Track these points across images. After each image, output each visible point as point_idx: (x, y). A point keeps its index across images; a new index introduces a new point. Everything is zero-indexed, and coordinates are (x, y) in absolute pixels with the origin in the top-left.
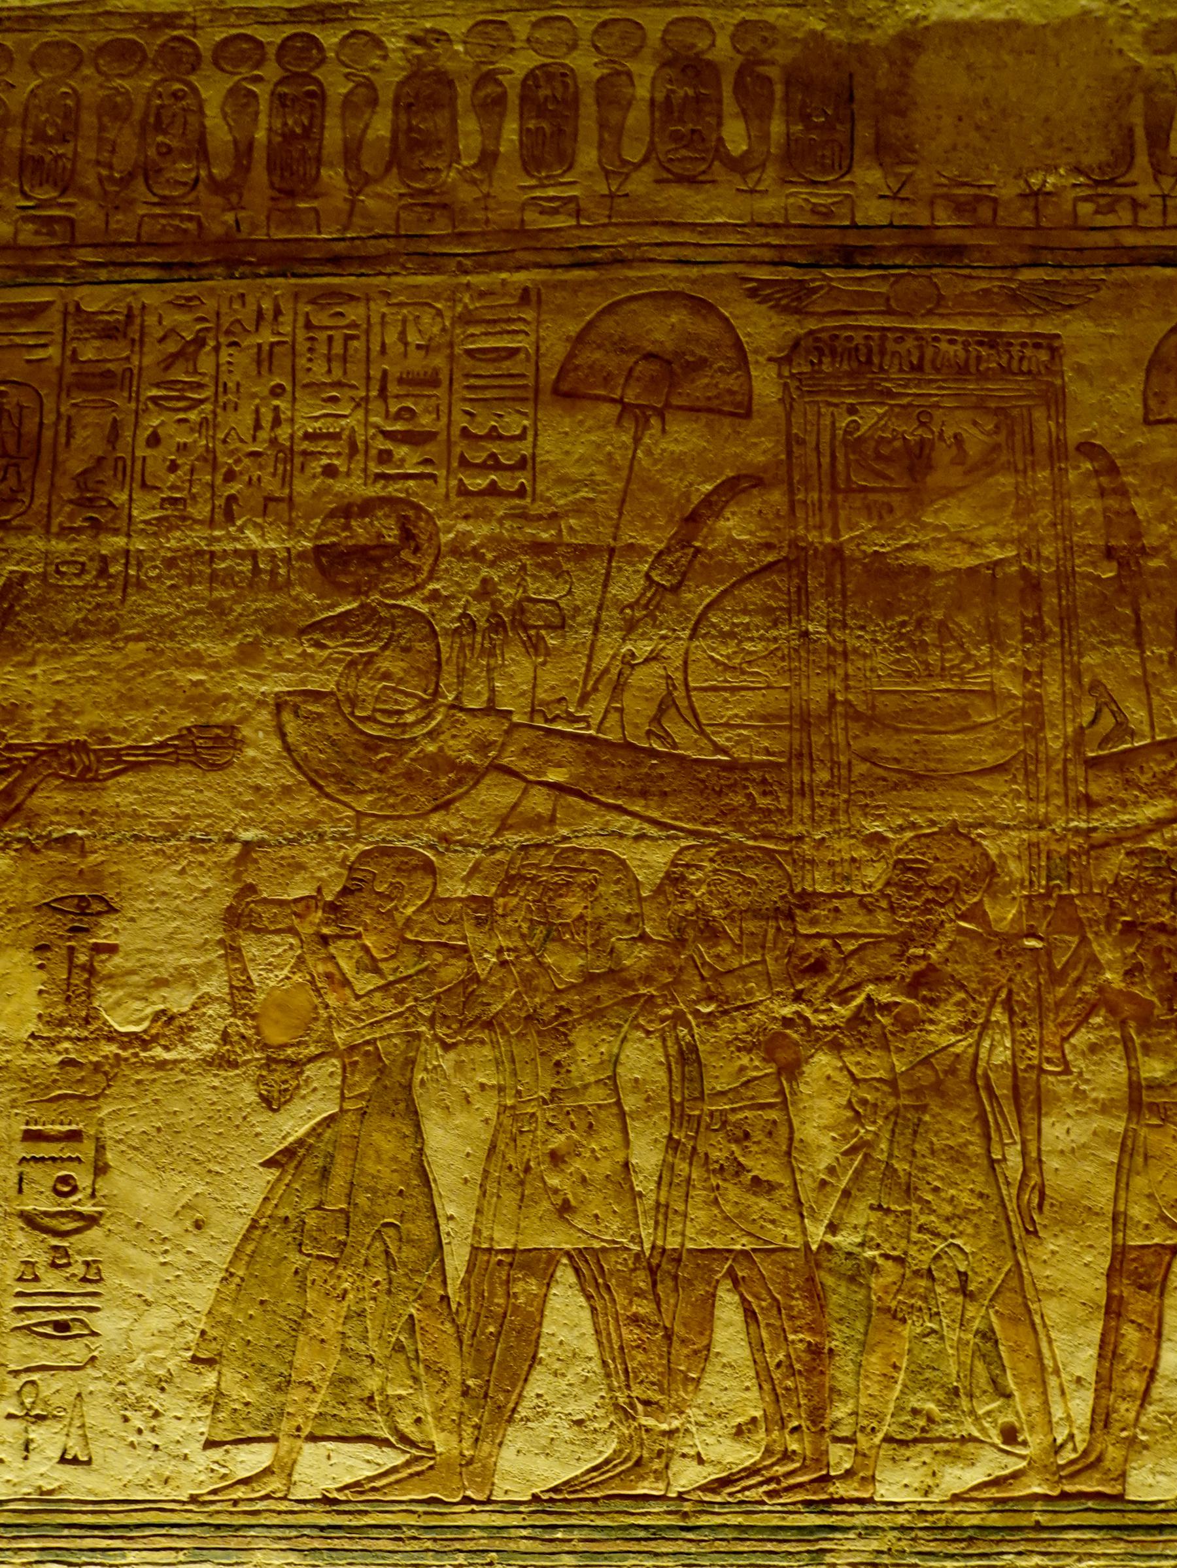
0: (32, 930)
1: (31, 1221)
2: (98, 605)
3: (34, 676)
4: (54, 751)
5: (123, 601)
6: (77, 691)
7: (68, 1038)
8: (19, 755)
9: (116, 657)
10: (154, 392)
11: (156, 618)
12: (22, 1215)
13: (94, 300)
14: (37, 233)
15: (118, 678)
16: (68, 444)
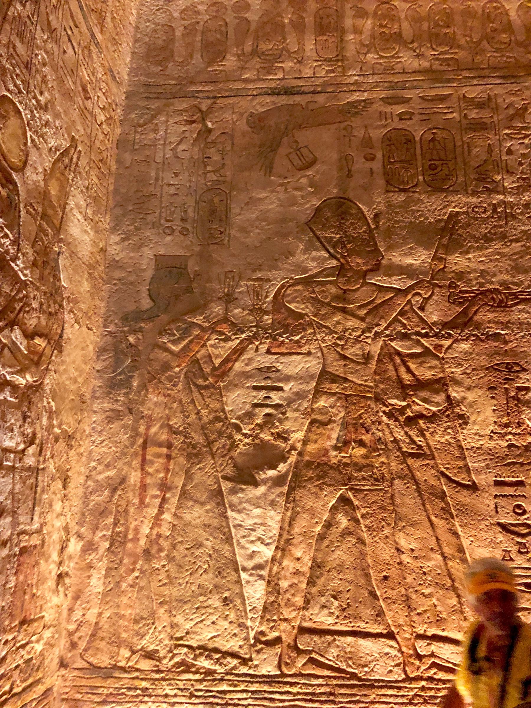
0: (486, 379)
1: (504, 527)
2: (495, 226)
3: (469, 259)
4: (483, 293)
5: (506, 224)
6: (491, 265)
7: (510, 433)
8: (467, 295)
9: (507, 250)
10: (507, 131)
11: (522, 231)
12: (499, 524)
13: (472, 93)
14: (441, 65)
15: (510, 259)
16: (469, 154)
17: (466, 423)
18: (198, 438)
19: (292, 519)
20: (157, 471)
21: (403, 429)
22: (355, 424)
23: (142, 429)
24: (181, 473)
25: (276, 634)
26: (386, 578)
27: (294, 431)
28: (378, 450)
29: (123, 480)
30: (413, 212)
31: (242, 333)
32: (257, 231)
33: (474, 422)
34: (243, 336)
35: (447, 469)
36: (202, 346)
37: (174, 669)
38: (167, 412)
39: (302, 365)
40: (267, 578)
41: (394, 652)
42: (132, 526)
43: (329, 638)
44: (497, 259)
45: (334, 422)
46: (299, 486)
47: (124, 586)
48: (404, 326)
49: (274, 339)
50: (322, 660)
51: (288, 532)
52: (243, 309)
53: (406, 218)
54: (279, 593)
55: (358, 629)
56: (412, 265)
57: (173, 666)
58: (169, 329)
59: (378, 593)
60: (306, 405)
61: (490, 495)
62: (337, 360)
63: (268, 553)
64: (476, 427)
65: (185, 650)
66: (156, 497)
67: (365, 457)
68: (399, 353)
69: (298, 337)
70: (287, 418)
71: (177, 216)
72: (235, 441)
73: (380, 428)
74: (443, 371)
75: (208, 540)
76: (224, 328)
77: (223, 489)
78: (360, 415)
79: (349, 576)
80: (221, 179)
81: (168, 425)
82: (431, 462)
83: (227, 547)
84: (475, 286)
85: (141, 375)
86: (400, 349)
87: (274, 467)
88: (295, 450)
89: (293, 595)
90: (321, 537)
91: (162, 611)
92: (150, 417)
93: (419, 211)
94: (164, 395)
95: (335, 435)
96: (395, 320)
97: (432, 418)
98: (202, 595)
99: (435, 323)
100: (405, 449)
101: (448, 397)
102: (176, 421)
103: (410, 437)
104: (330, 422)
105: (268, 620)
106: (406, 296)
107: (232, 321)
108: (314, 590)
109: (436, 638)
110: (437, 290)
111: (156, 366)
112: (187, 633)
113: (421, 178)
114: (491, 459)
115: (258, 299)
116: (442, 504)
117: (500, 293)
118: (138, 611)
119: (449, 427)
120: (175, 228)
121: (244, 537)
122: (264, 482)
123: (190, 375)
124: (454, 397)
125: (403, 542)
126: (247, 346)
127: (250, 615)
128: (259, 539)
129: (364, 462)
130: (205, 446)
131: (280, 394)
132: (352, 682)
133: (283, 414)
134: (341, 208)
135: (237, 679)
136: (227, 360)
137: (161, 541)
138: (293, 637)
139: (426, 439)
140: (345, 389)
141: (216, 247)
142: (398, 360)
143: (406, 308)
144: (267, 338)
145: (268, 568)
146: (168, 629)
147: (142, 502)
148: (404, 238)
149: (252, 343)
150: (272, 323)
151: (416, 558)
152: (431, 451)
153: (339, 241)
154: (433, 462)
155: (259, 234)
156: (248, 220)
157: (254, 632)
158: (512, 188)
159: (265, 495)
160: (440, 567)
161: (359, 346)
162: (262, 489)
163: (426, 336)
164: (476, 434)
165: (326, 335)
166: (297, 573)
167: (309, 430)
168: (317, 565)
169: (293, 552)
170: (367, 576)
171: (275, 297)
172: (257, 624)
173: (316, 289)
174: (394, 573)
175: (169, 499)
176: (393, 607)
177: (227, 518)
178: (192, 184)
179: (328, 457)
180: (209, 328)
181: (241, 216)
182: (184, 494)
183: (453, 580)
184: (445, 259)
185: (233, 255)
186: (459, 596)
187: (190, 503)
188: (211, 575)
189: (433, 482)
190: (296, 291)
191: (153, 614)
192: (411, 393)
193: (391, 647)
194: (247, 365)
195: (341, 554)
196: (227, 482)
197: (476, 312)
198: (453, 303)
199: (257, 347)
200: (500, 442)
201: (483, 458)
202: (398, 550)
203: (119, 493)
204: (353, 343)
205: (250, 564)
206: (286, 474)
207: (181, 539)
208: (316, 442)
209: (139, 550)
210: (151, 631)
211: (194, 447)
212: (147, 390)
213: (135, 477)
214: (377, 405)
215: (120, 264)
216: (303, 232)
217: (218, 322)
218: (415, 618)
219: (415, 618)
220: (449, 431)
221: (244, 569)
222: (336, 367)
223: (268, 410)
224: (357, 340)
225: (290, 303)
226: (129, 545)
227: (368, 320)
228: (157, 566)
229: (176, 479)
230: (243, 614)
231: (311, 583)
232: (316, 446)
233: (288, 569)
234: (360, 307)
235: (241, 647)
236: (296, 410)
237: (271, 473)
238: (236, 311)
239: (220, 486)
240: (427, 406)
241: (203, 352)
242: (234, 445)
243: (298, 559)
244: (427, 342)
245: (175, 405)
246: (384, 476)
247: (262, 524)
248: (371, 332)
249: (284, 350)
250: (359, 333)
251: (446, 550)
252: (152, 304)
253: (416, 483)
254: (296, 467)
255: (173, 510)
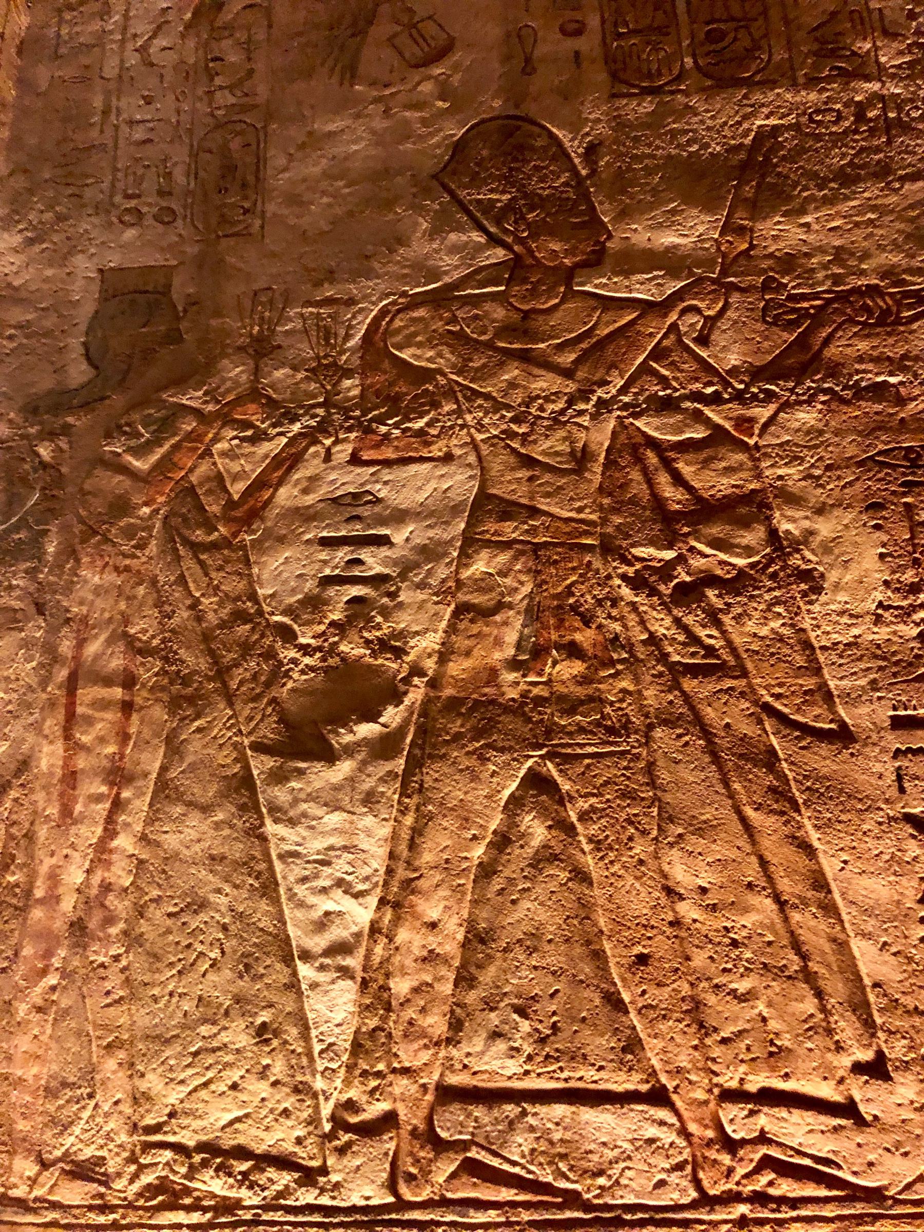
0: (858, 486)
2: (863, 149)
3: (807, 225)
5: (889, 142)
6: (859, 234)
9: (893, 199)
12: (909, 818)
15: (900, 218)
17: (818, 590)
18: (193, 660)
19: (417, 832)
20: (102, 740)
21: (670, 612)
22: (559, 607)
23: (66, 647)
24: (156, 741)
25: (382, 1107)
26: (642, 959)
27: (417, 633)
28: (612, 663)
29: (24, 765)
30: (674, 134)
31: (292, 421)
32: (325, 200)
33: (837, 586)
34: (296, 427)
35: (778, 697)
36: (201, 457)
37: (141, 1202)
38: (123, 605)
39: (433, 484)
40: (359, 975)
41: (668, 1137)
42: (44, 869)
43: (511, 1110)
44: (871, 221)
45: (510, 606)
46: (431, 756)
47: (22, 1009)
48: (664, 382)
49: (368, 431)
50: (495, 1162)
51: (408, 863)
52: (295, 368)
53: (658, 148)
54: (388, 1008)
55: (580, 1085)
56: (676, 247)
57: (140, 1195)
58: (128, 425)
59: (626, 997)
60: (442, 572)
61: (884, 750)
62: (513, 469)
63: (361, 914)
64: (842, 597)
65: (168, 1155)
66: (99, 798)
67: (584, 680)
68: (652, 443)
69: (421, 423)
70: (400, 605)
71: (150, 185)
72: (281, 664)
73: (614, 612)
74: (759, 476)
75: (219, 891)
76: (254, 414)
77: (255, 772)
78: (569, 587)
79: (554, 959)
80: (245, 100)
81: (125, 634)
82: (740, 683)
83: (264, 905)
84: (822, 283)
85: (65, 529)
86: (656, 434)
87: (372, 716)
88: (421, 673)
89: (423, 1010)
90: (486, 871)
91: (111, 1064)
92: (84, 620)
93: (686, 132)
94: (116, 569)
95: (511, 637)
96: (644, 369)
97: (738, 583)
98: (205, 1021)
99: (734, 371)
100: (676, 658)
101: (773, 533)
102: (144, 627)
103: (686, 629)
104: (500, 606)
105: (365, 1074)
106: (666, 315)
107: (269, 398)
108: (472, 997)
109: (770, 1097)
110: (735, 298)
111: (99, 506)
112: (171, 1115)
113: (688, 61)
114: (880, 668)
115: (328, 343)
116: (770, 780)
117: (882, 295)
118: (55, 1067)
119: (777, 602)
120: (145, 210)
121: (304, 880)
122: (349, 751)
123: (176, 521)
124: (787, 532)
125: (681, 873)
126: (306, 449)
127: (320, 1065)
128: (340, 883)
129: (580, 692)
130: (210, 679)
131: (384, 552)
132: (568, 1214)
133: (392, 595)
134: (511, 139)
135: (292, 1218)
136: (260, 484)
137: (111, 900)
138: (423, 1113)
139: (724, 633)
140: (533, 531)
141: (232, 241)
142: (652, 458)
143: (666, 343)
144: (349, 430)
145: (362, 951)
146: (126, 1108)
147: (66, 812)
148: (654, 192)
149: (316, 442)
150: (362, 395)
151: (714, 908)
152: (737, 657)
153: (509, 207)
154: (744, 682)
155: (330, 205)
156: (304, 180)
157: (332, 1103)
158: (899, 67)
159: (351, 780)
160: (771, 928)
161: (561, 433)
162: (345, 767)
163: (715, 400)
164: (841, 613)
165: (486, 413)
166: (430, 958)
167: (452, 629)
168: (477, 938)
169: (419, 909)
170: (598, 956)
171: (365, 338)
172: (338, 1083)
173: (460, 314)
174: (660, 946)
175: (128, 801)
176: (663, 1027)
177: (263, 839)
178: (183, 117)
179: (499, 686)
180: (217, 415)
181: (285, 171)
182: (165, 790)
183: (804, 957)
184: (752, 230)
185: (274, 255)
186: (819, 994)
187: (179, 810)
188: (227, 974)
189: (747, 728)
190: (414, 320)
191: (90, 1072)
192: (686, 530)
193: (662, 1123)
194: (305, 491)
195: (535, 909)
196: (263, 757)
197: (827, 341)
198: (774, 324)
199: (328, 451)
200: (901, 627)
201: (863, 665)
202: (669, 891)
203: (13, 794)
204: (548, 428)
205: (317, 943)
206: (401, 731)
207: (155, 893)
208: (468, 654)
209: (59, 925)
210: (86, 1114)
211: (186, 681)
212: (78, 561)
213: (49, 757)
214: (606, 562)
215: (23, 294)
216: (427, 192)
217: (239, 401)
218: (716, 1052)
219: (716, 1052)
220: (778, 609)
221: (306, 956)
222: (512, 485)
223: (356, 591)
224: (556, 421)
225: (400, 348)
226: (37, 914)
227: (580, 374)
228: (101, 959)
229: (144, 756)
230: (305, 1061)
231: (465, 980)
232: (467, 663)
233: (409, 951)
234: (560, 348)
235: (299, 1141)
236: (422, 586)
237: (366, 730)
238: (279, 374)
239: (247, 768)
240: (722, 556)
241: (204, 468)
242: (278, 674)
243: (433, 925)
244: (719, 413)
245: (141, 590)
246: (629, 721)
247: (345, 848)
248: (588, 400)
249: (390, 454)
250: (561, 405)
251: (785, 885)
252: (90, 373)
253: (706, 733)
254: (424, 713)
255: (138, 828)
